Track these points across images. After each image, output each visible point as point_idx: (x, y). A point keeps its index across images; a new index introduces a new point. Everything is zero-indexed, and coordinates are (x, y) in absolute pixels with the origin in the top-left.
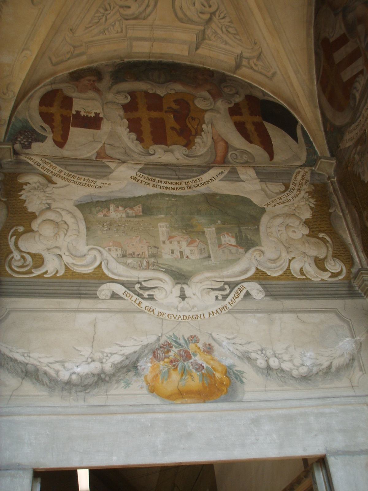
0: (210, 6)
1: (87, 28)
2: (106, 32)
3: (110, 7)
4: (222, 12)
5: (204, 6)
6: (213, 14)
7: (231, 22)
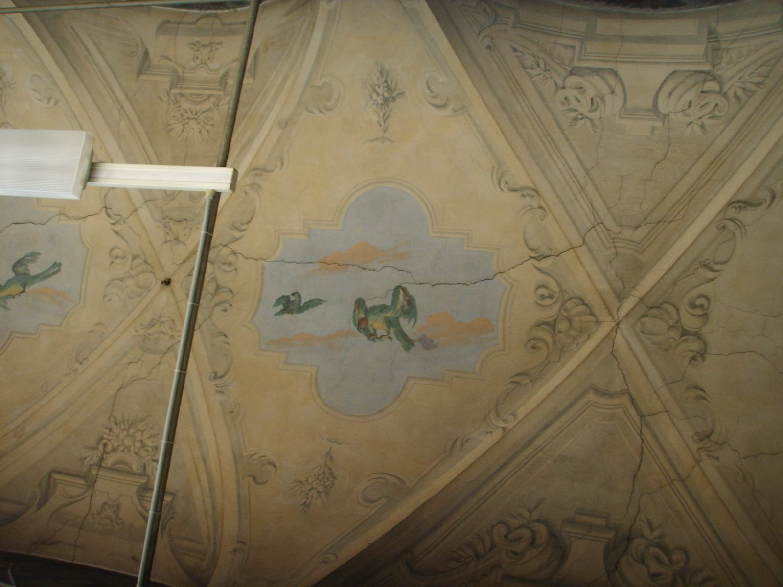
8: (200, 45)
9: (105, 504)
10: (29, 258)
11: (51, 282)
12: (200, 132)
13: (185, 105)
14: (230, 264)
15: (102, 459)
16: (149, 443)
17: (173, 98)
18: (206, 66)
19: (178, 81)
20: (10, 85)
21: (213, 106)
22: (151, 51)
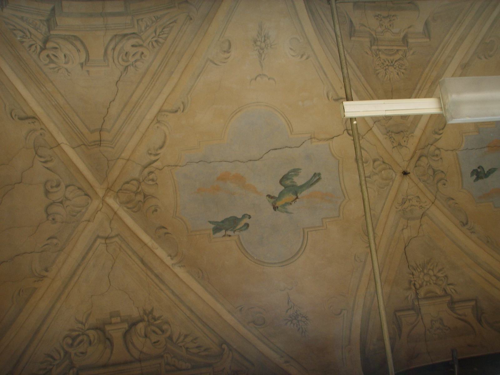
0: (48, 56)
1: (175, 22)
2: (154, 19)
3: (153, 45)
4: (34, 52)
5: (54, 55)
6: (43, 49)
7: (22, 42)
8: (382, 17)
9: (432, 321)
10: (293, 173)
11: (317, 187)
12: (398, 74)
13: (383, 57)
14: (437, 156)
15: (417, 294)
16: (439, 275)
17: (374, 52)
18: (389, 31)
19: (374, 41)
20: (271, 46)
21: (402, 57)
22: (353, 20)
